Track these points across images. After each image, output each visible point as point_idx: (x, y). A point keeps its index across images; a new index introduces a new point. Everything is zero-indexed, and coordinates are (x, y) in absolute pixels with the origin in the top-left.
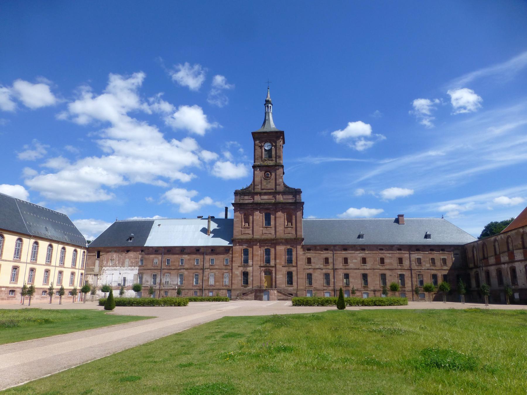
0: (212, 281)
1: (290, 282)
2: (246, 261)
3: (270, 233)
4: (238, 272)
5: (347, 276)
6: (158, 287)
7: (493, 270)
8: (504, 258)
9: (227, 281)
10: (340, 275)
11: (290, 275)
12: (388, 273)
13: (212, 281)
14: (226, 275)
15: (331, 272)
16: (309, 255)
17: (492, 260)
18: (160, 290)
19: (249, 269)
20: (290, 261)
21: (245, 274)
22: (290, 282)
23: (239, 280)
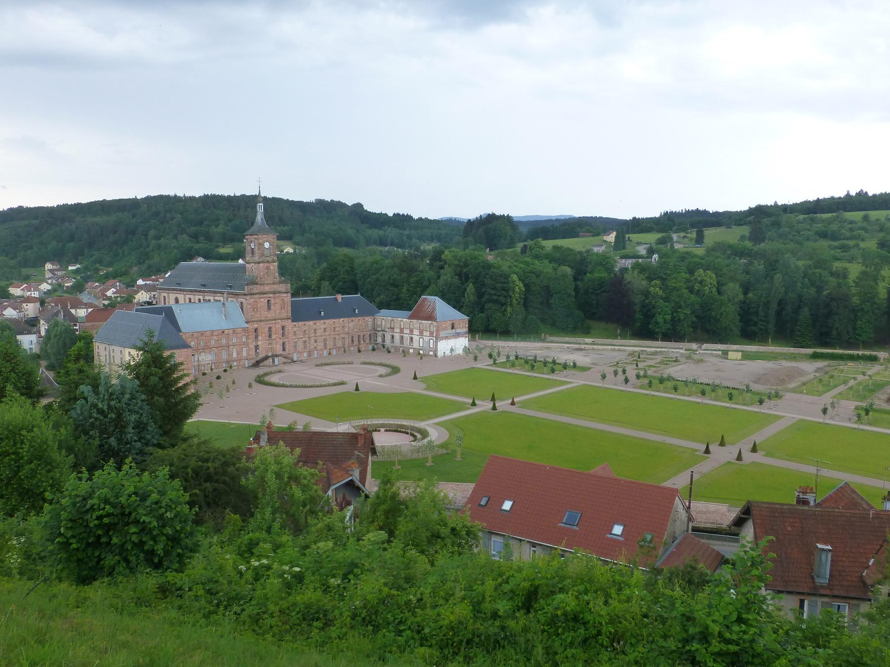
0: (235, 355)
1: (284, 350)
2: (256, 337)
3: (271, 315)
4: (252, 346)
5: (316, 341)
6: (196, 364)
7: (397, 337)
8: (406, 331)
9: (245, 354)
10: (313, 339)
11: (284, 344)
12: (337, 337)
13: (235, 355)
14: (244, 349)
15: (306, 339)
16: (295, 329)
17: (397, 330)
18: (199, 366)
19: (260, 343)
20: (283, 335)
21: (257, 347)
22: (284, 350)
23: (253, 352)
